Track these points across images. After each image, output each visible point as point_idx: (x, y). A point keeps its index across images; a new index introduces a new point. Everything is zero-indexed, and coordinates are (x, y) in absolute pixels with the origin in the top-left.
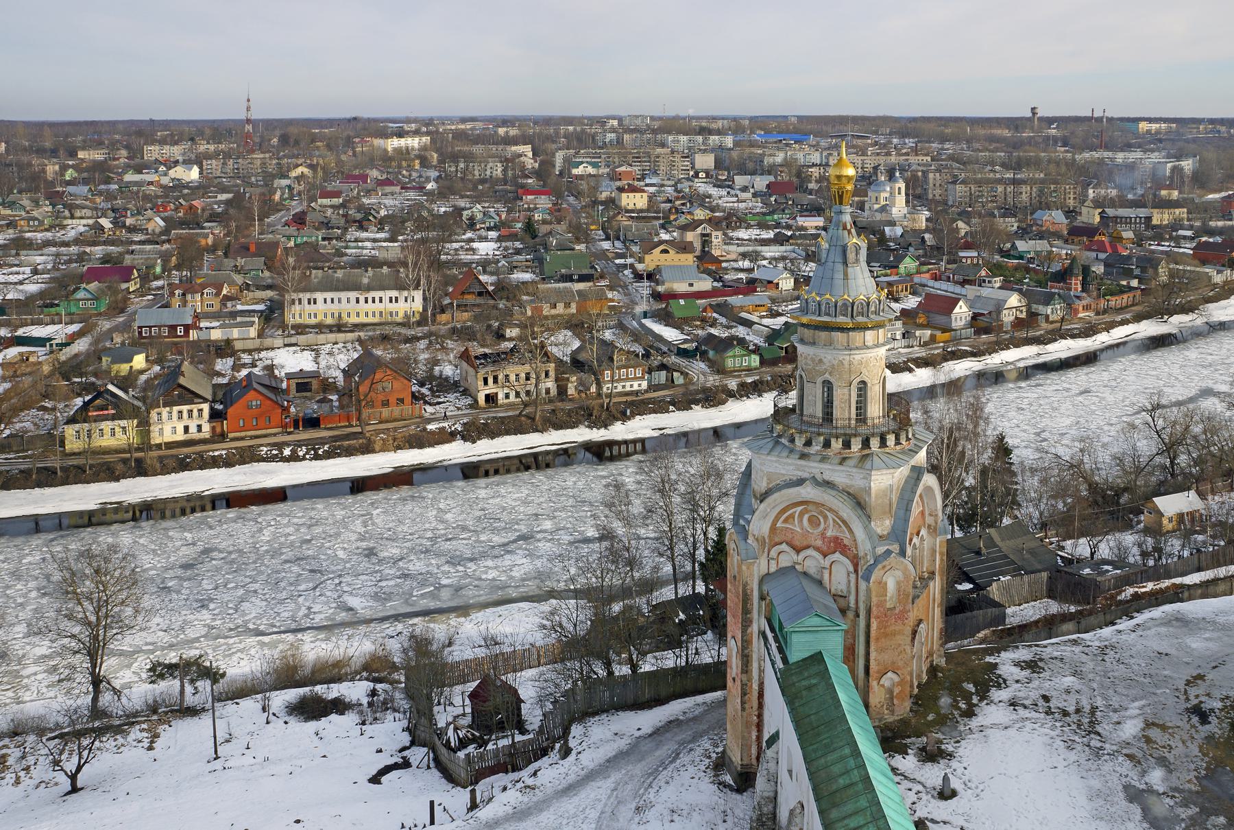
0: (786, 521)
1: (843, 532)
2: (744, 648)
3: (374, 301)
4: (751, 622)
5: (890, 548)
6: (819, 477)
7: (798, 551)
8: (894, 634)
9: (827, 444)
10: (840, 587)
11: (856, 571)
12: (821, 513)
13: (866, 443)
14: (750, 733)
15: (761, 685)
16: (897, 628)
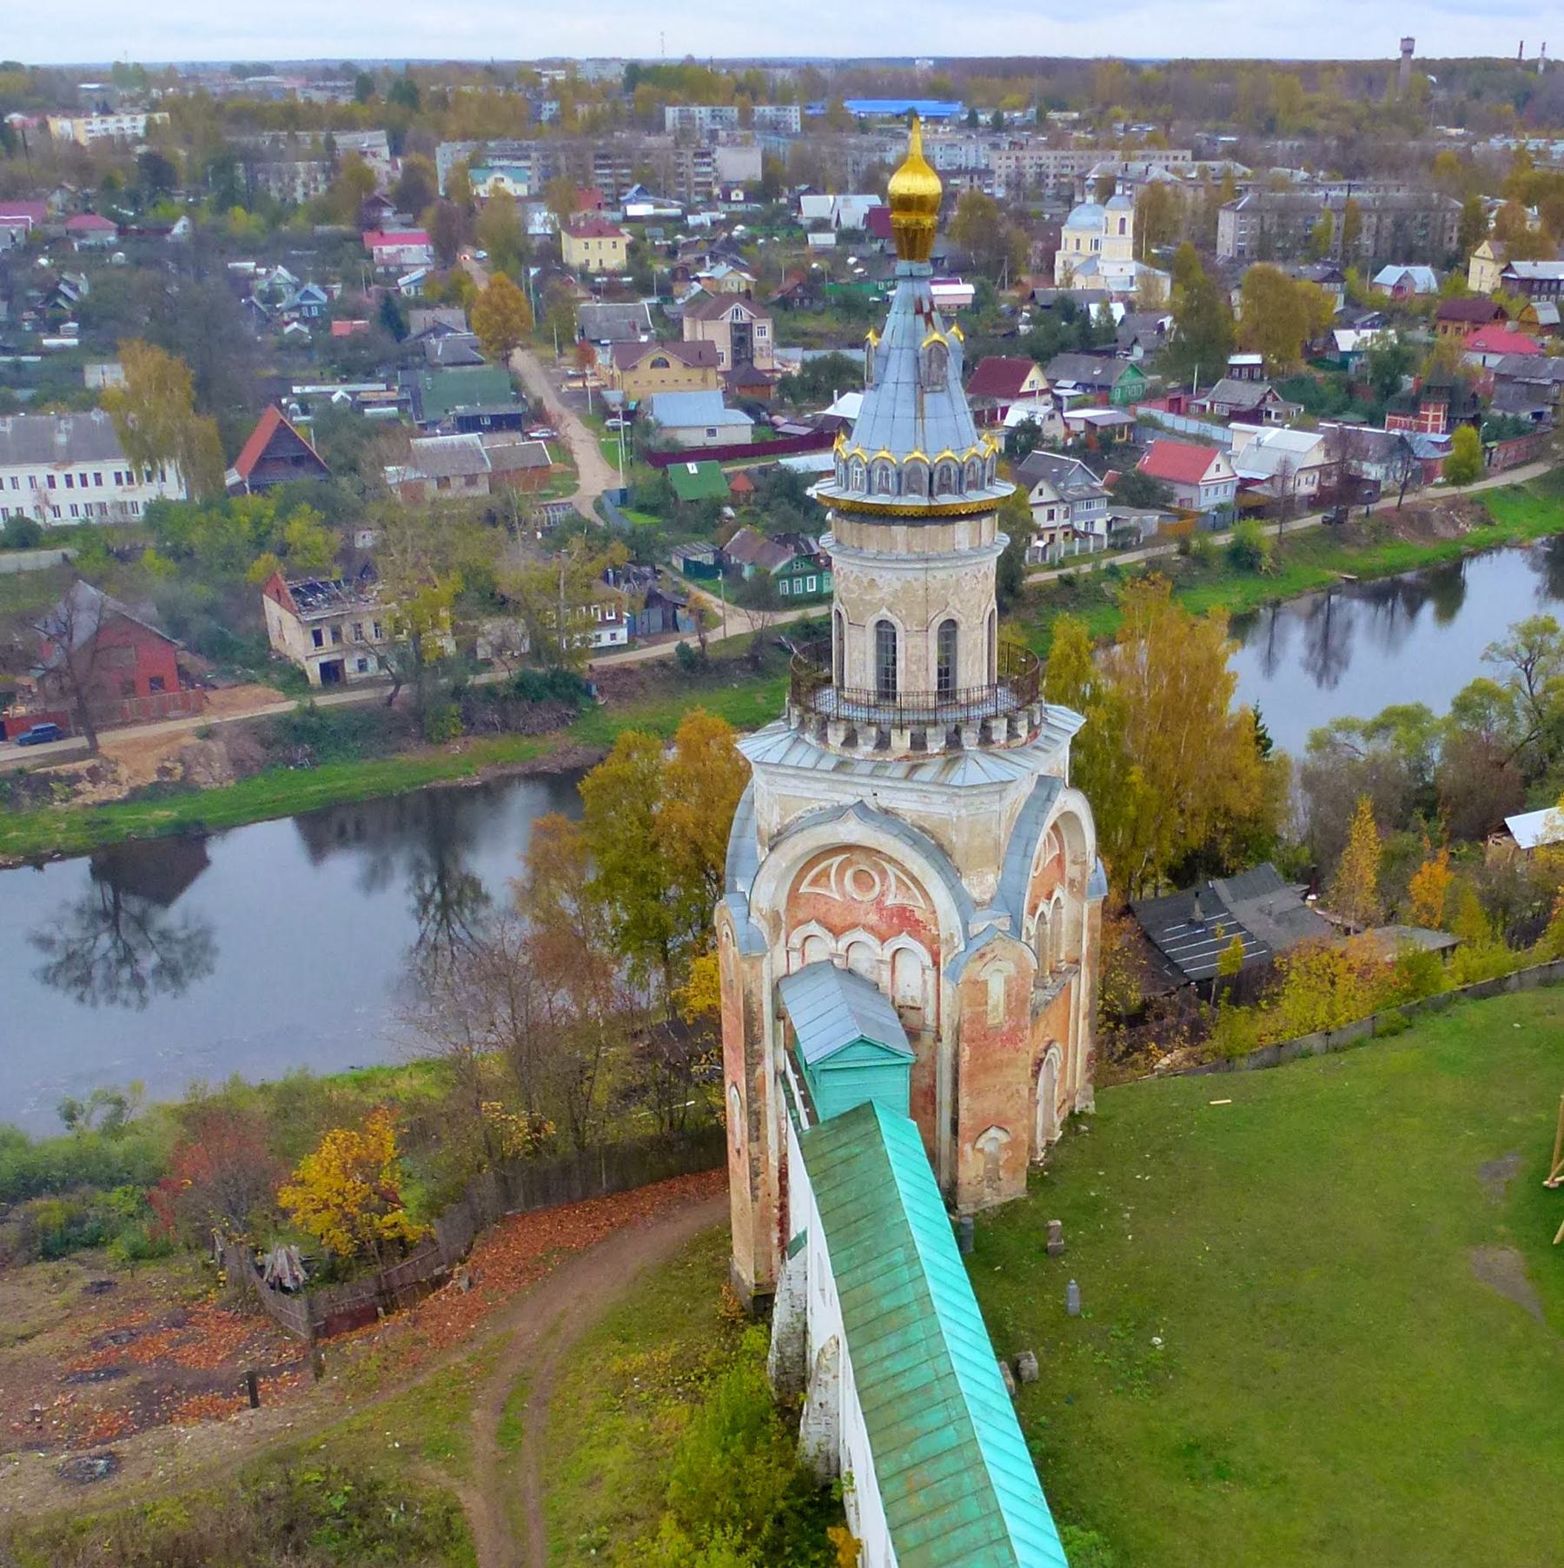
0: (814, 882)
1: (914, 897)
2: (751, 1101)
3: (84, 483)
4: (761, 1057)
5: (996, 923)
6: (871, 803)
7: (836, 932)
8: (1000, 1066)
9: (883, 743)
10: (910, 993)
11: (936, 963)
12: (876, 864)
13: (954, 741)
14: (768, 1235)
15: (783, 1157)
16: (1005, 1056)
